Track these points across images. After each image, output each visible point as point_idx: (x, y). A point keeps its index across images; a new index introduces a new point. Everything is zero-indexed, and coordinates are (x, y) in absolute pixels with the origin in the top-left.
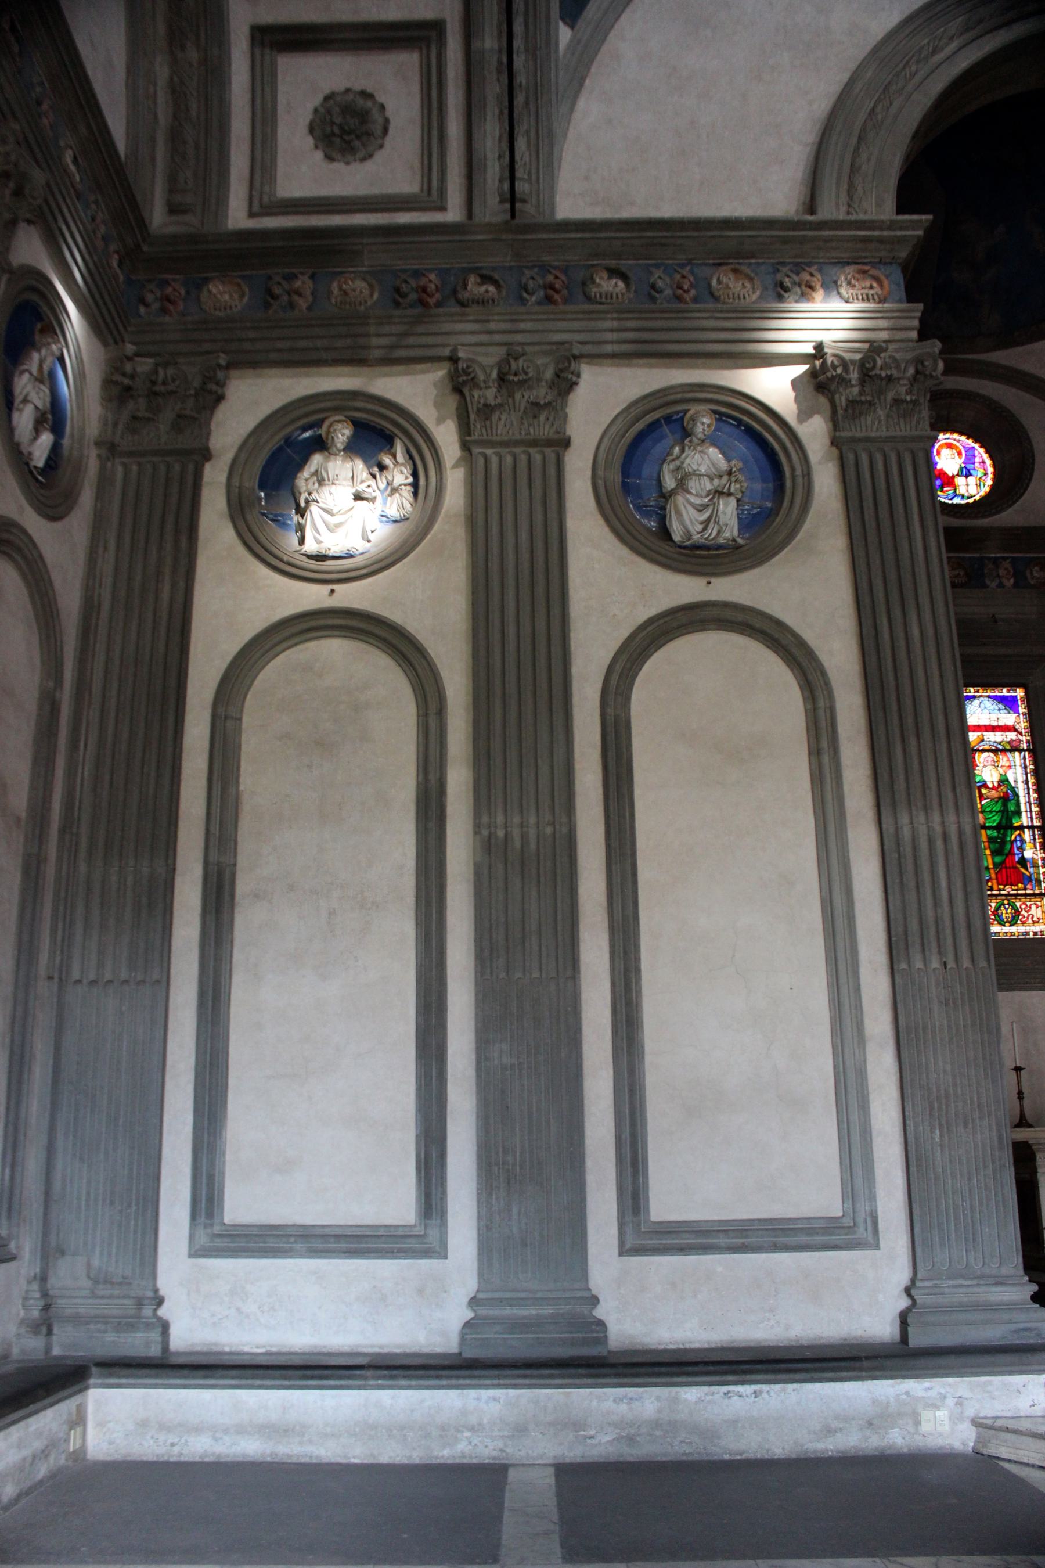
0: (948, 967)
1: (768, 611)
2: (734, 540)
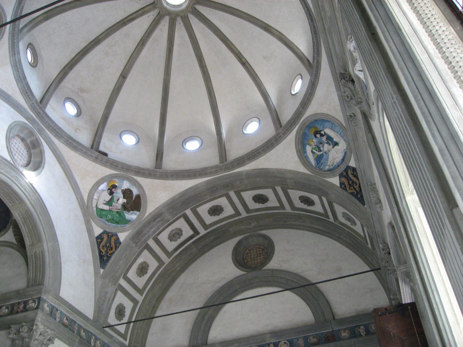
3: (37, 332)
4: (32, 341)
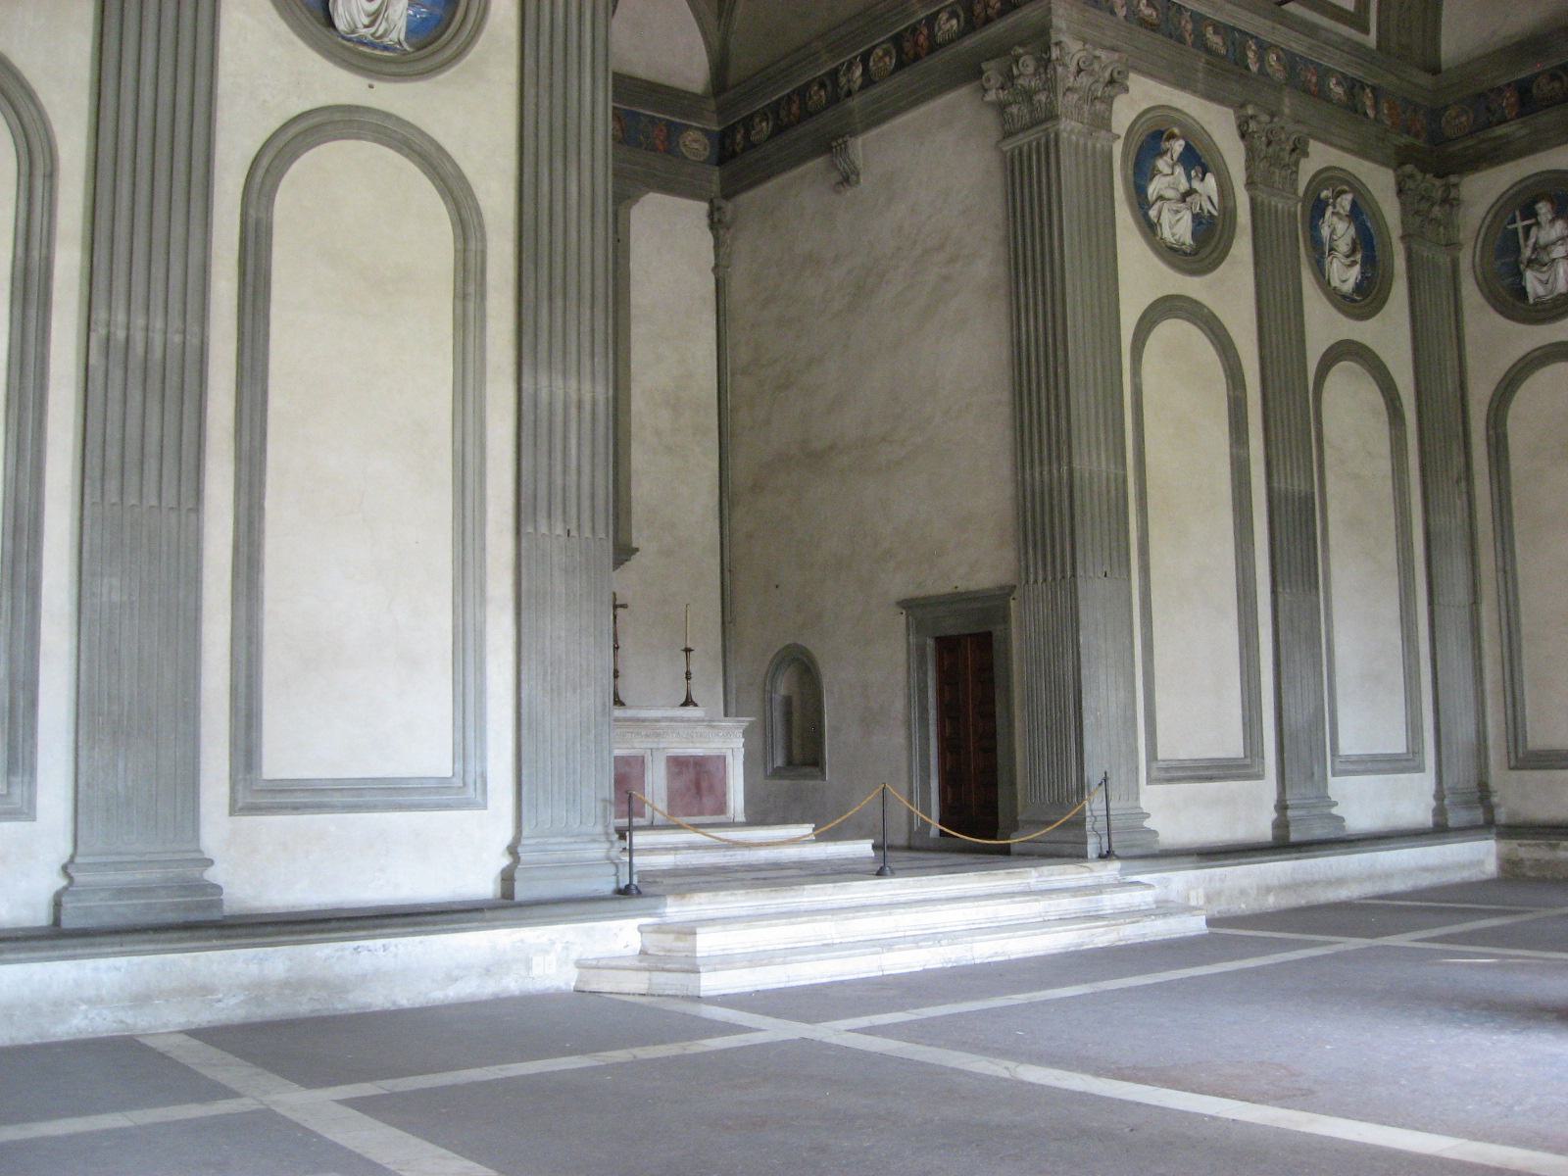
0: (572, 534)
1: (429, 132)
2: (400, 43)
3: (1065, 65)
4: (1060, 98)
